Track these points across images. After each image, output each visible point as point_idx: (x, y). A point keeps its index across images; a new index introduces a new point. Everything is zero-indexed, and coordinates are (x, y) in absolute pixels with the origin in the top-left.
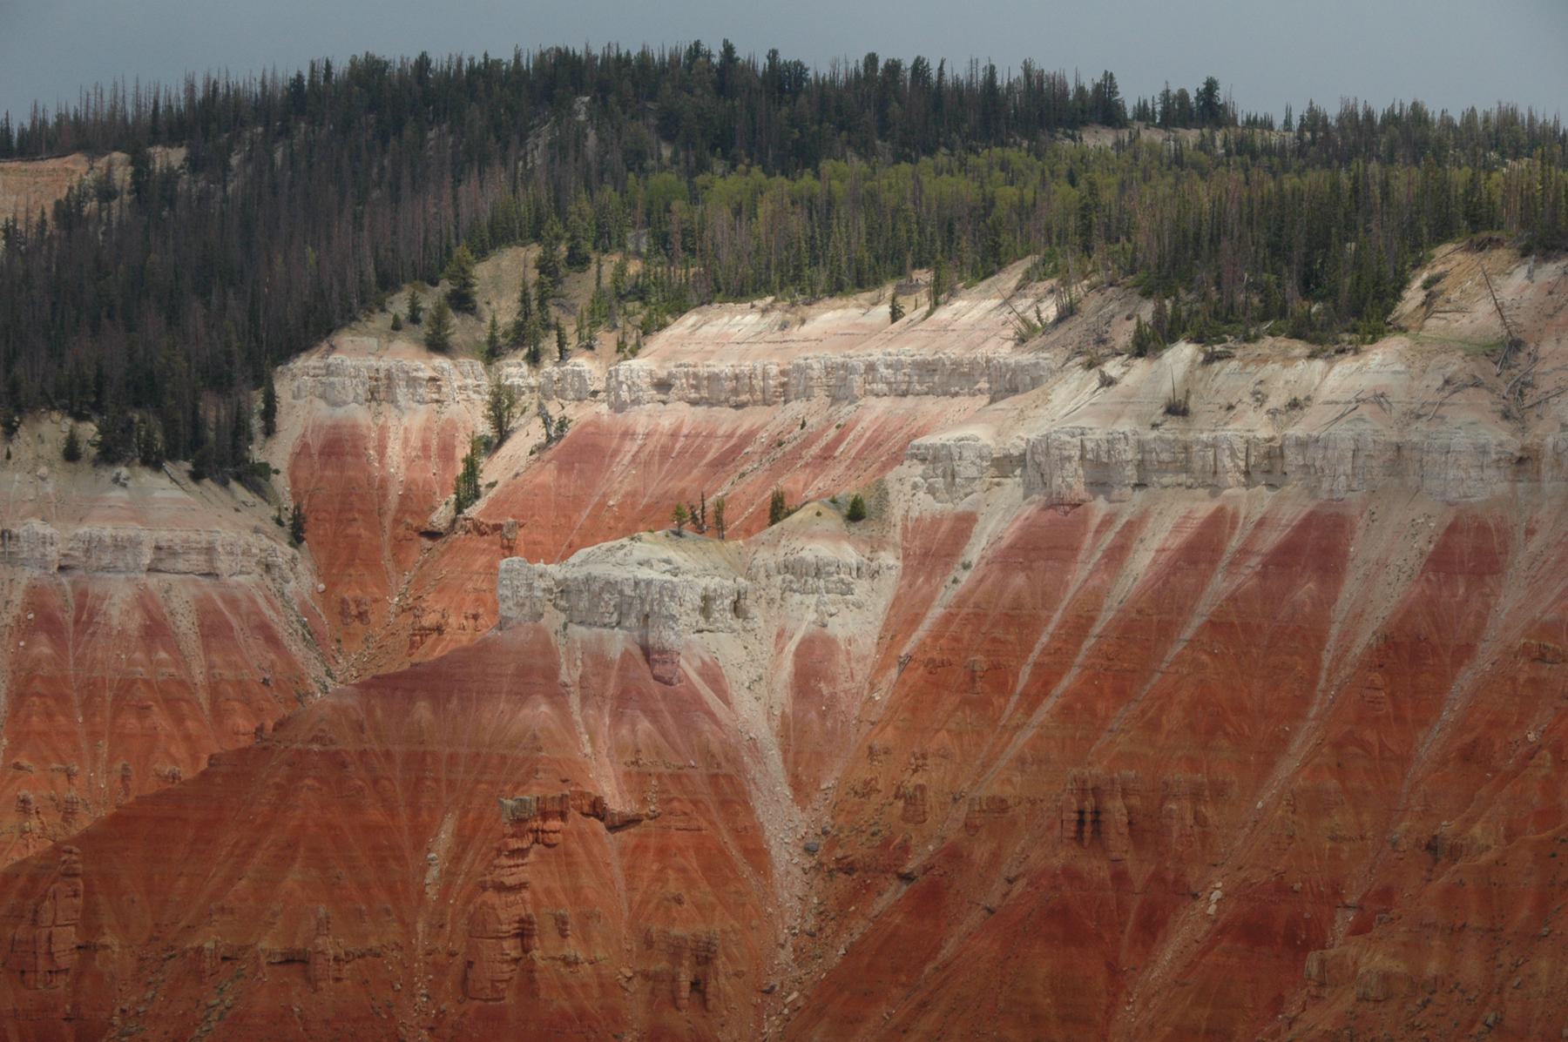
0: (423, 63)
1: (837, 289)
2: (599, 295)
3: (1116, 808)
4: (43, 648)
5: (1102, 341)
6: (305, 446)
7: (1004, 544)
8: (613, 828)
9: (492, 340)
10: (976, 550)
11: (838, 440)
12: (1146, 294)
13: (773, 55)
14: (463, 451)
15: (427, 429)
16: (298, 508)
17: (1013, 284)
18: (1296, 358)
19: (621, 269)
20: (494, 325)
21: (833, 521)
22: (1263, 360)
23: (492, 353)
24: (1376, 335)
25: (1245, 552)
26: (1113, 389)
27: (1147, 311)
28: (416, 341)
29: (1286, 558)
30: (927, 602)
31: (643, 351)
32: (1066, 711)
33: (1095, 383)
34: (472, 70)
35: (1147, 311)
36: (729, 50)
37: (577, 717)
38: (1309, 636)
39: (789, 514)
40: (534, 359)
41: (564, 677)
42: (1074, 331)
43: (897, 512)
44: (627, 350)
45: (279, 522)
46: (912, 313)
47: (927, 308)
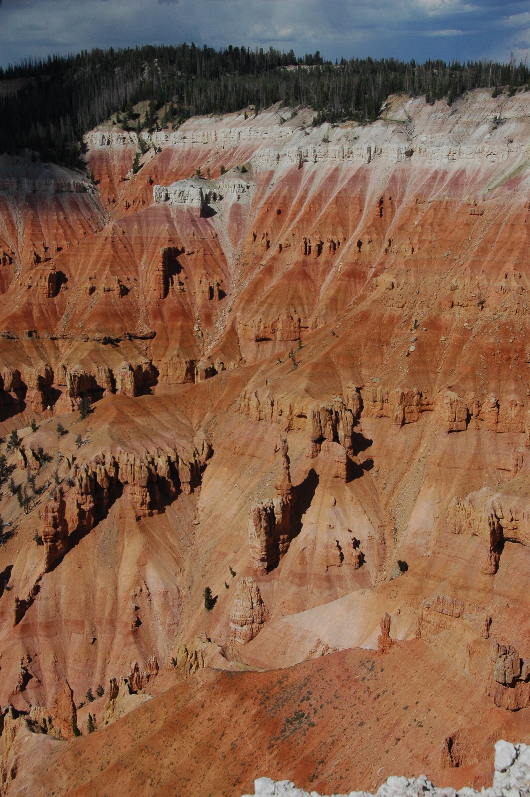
0: (112, 50)
1: (230, 111)
2: (166, 115)
3: (313, 245)
4: (31, 212)
5: (304, 123)
6: (93, 157)
7: (283, 178)
8: (188, 255)
9: (139, 126)
10: (275, 180)
11: (234, 152)
12: (315, 110)
13: (205, 46)
14: (134, 157)
15: (124, 151)
16: (92, 173)
17: (277, 108)
18: (354, 127)
19: (172, 106)
20: (139, 122)
21: (238, 173)
22: (346, 127)
23: (138, 130)
24: (376, 119)
25: (344, 177)
26: (308, 136)
27: (316, 114)
28: (119, 128)
29: (355, 179)
30: (263, 194)
31: (179, 129)
32: (301, 220)
33: (304, 134)
34: (126, 52)
35: (316, 114)
36: (193, 45)
37: (176, 226)
38: (361, 199)
39: (227, 171)
40: (151, 131)
41: (172, 216)
42: (297, 120)
43: (254, 171)
44: (175, 128)
45: (88, 178)
46: (250, 118)
47: (254, 115)
